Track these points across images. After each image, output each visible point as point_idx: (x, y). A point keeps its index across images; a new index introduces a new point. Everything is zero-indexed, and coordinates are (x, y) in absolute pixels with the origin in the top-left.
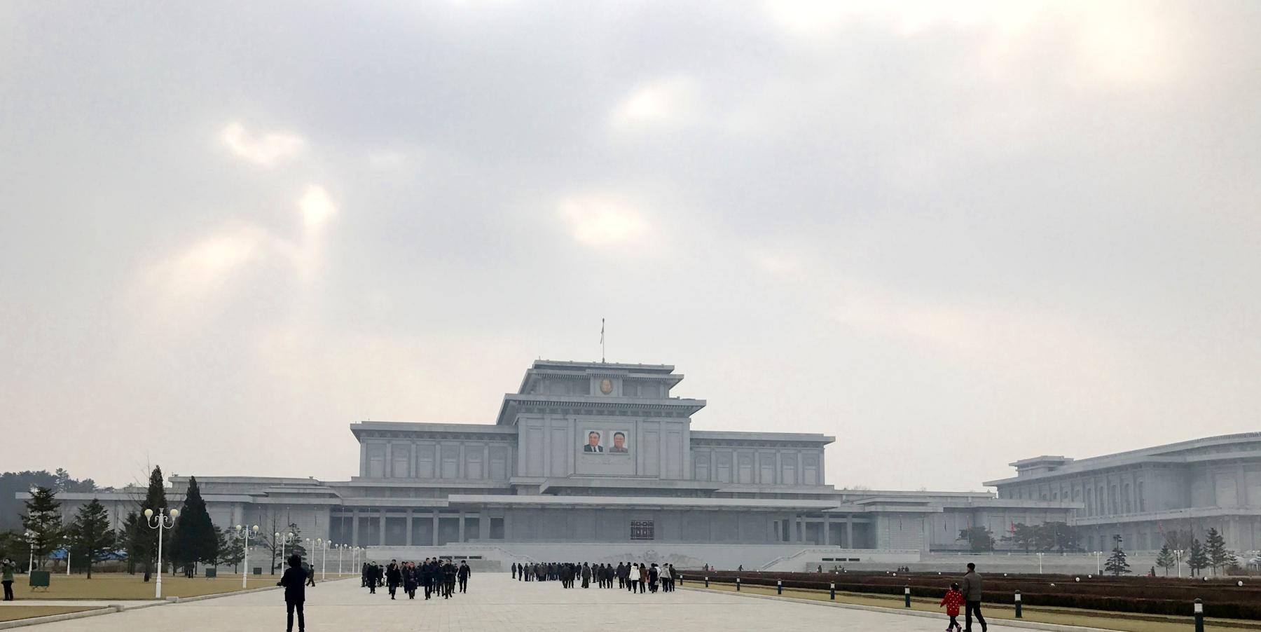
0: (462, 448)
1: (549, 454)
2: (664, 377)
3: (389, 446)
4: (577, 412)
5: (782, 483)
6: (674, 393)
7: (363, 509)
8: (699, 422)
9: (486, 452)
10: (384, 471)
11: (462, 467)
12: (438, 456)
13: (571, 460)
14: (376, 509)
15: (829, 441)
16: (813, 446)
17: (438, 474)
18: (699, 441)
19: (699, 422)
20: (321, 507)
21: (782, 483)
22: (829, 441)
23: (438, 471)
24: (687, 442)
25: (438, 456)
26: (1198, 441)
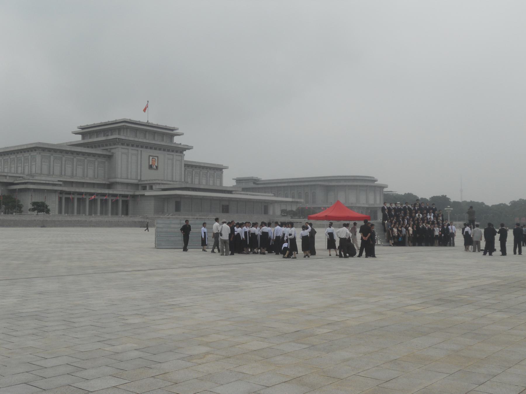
0: (86, 160)
2: (168, 133)
3: (52, 157)
4: (142, 147)
5: (65, 175)
6: (177, 140)
7: (91, 194)
8: (189, 156)
9: (96, 164)
10: (73, 173)
11: (52, 168)
13: (139, 171)
14: (74, 193)
15: (226, 168)
16: (218, 170)
17: (51, 173)
18: (190, 166)
19: (189, 156)
20: (55, 191)
21: (65, 175)
22: (226, 168)
24: (183, 166)
25: (75, 164)
26: (338, 176)
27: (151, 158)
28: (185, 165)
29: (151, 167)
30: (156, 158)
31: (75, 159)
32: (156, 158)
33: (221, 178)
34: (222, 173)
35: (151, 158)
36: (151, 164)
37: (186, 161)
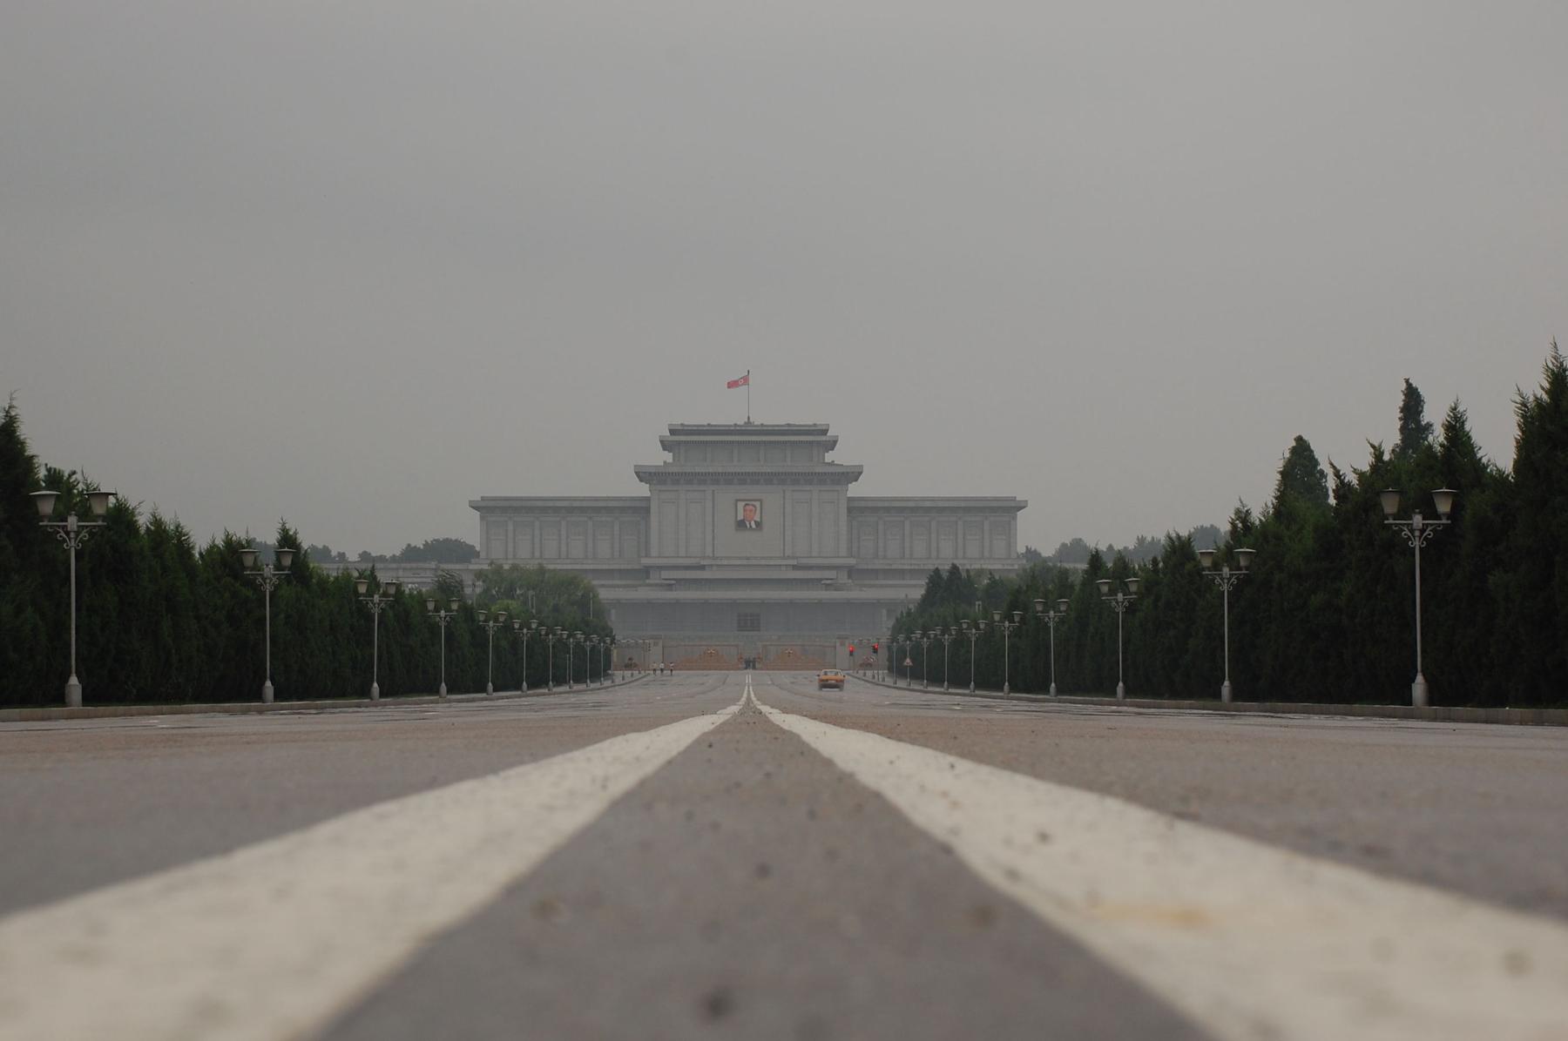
1: (696, 533)
2: (817, 439)
6: (829, 457)
8: (854, 490)
12: (563, 532)
19: (854, 490)
23: (564, 549)
24: (843, 510)
25: (563, 532)
27: (741, 505)
28: (850, 510)
29: (741, 525)
30: (757, 504)
31: (907, 523)
32: (757, 504)
33: (1009, 531)
34: (1015, 518)
35: (741, 505)
36: (740, 517)
37: (850, 499)
